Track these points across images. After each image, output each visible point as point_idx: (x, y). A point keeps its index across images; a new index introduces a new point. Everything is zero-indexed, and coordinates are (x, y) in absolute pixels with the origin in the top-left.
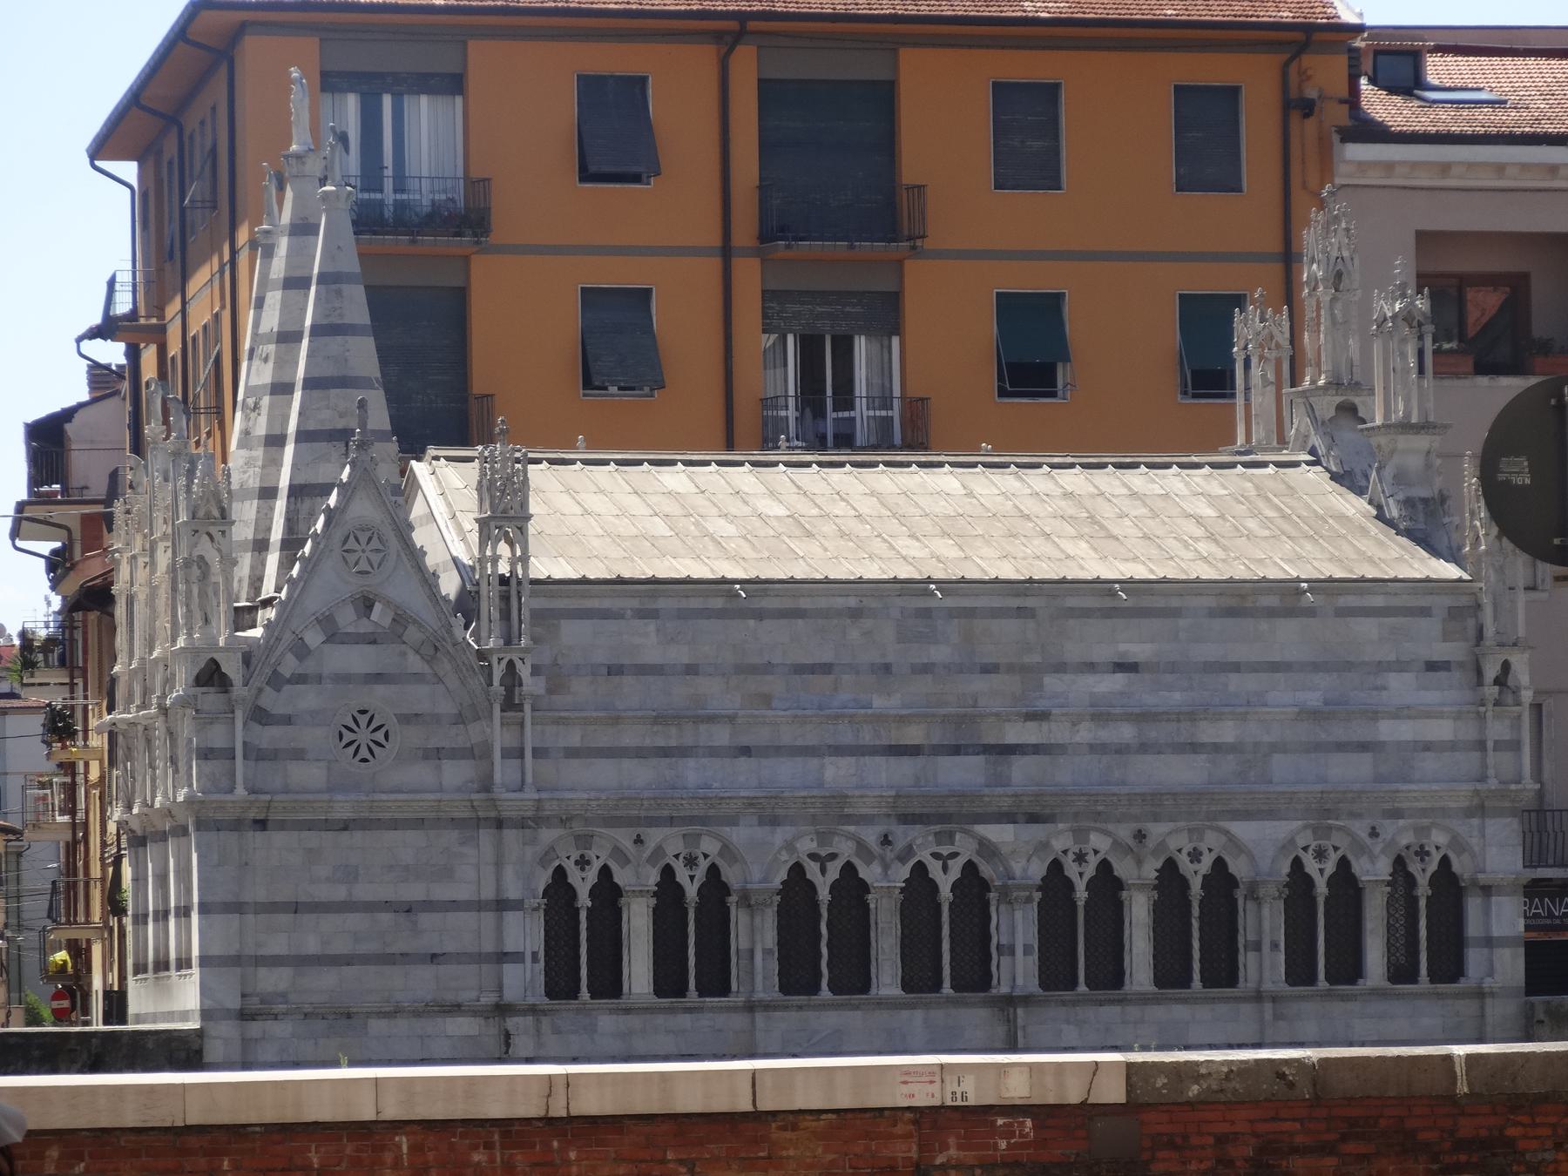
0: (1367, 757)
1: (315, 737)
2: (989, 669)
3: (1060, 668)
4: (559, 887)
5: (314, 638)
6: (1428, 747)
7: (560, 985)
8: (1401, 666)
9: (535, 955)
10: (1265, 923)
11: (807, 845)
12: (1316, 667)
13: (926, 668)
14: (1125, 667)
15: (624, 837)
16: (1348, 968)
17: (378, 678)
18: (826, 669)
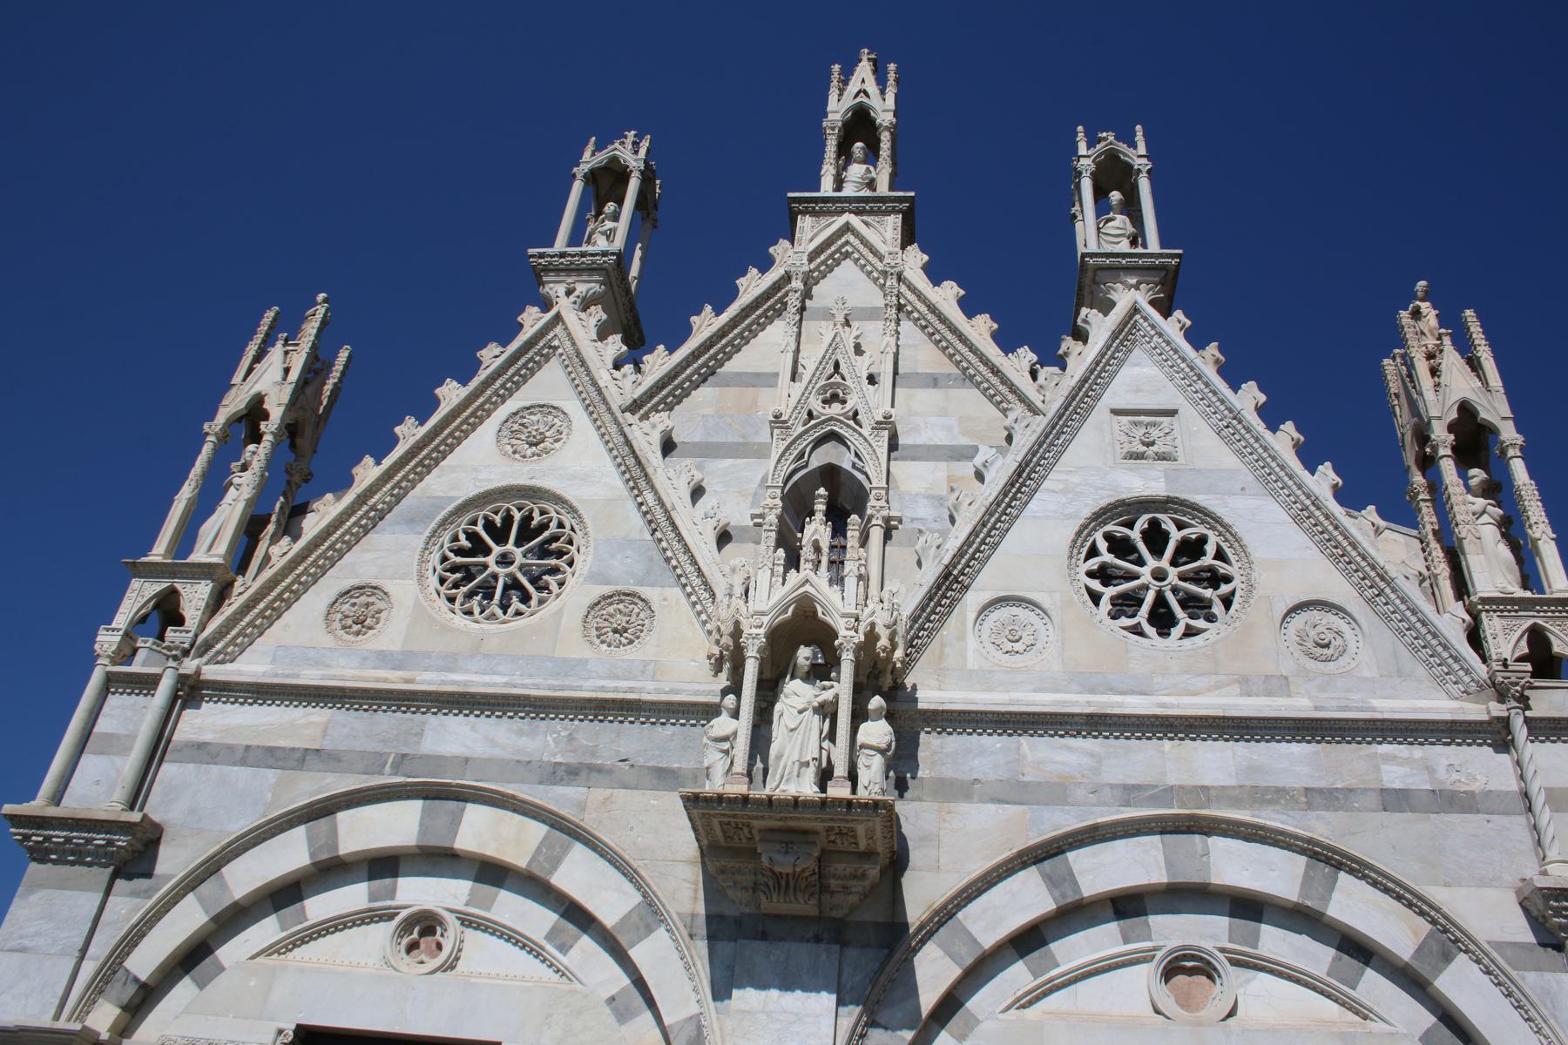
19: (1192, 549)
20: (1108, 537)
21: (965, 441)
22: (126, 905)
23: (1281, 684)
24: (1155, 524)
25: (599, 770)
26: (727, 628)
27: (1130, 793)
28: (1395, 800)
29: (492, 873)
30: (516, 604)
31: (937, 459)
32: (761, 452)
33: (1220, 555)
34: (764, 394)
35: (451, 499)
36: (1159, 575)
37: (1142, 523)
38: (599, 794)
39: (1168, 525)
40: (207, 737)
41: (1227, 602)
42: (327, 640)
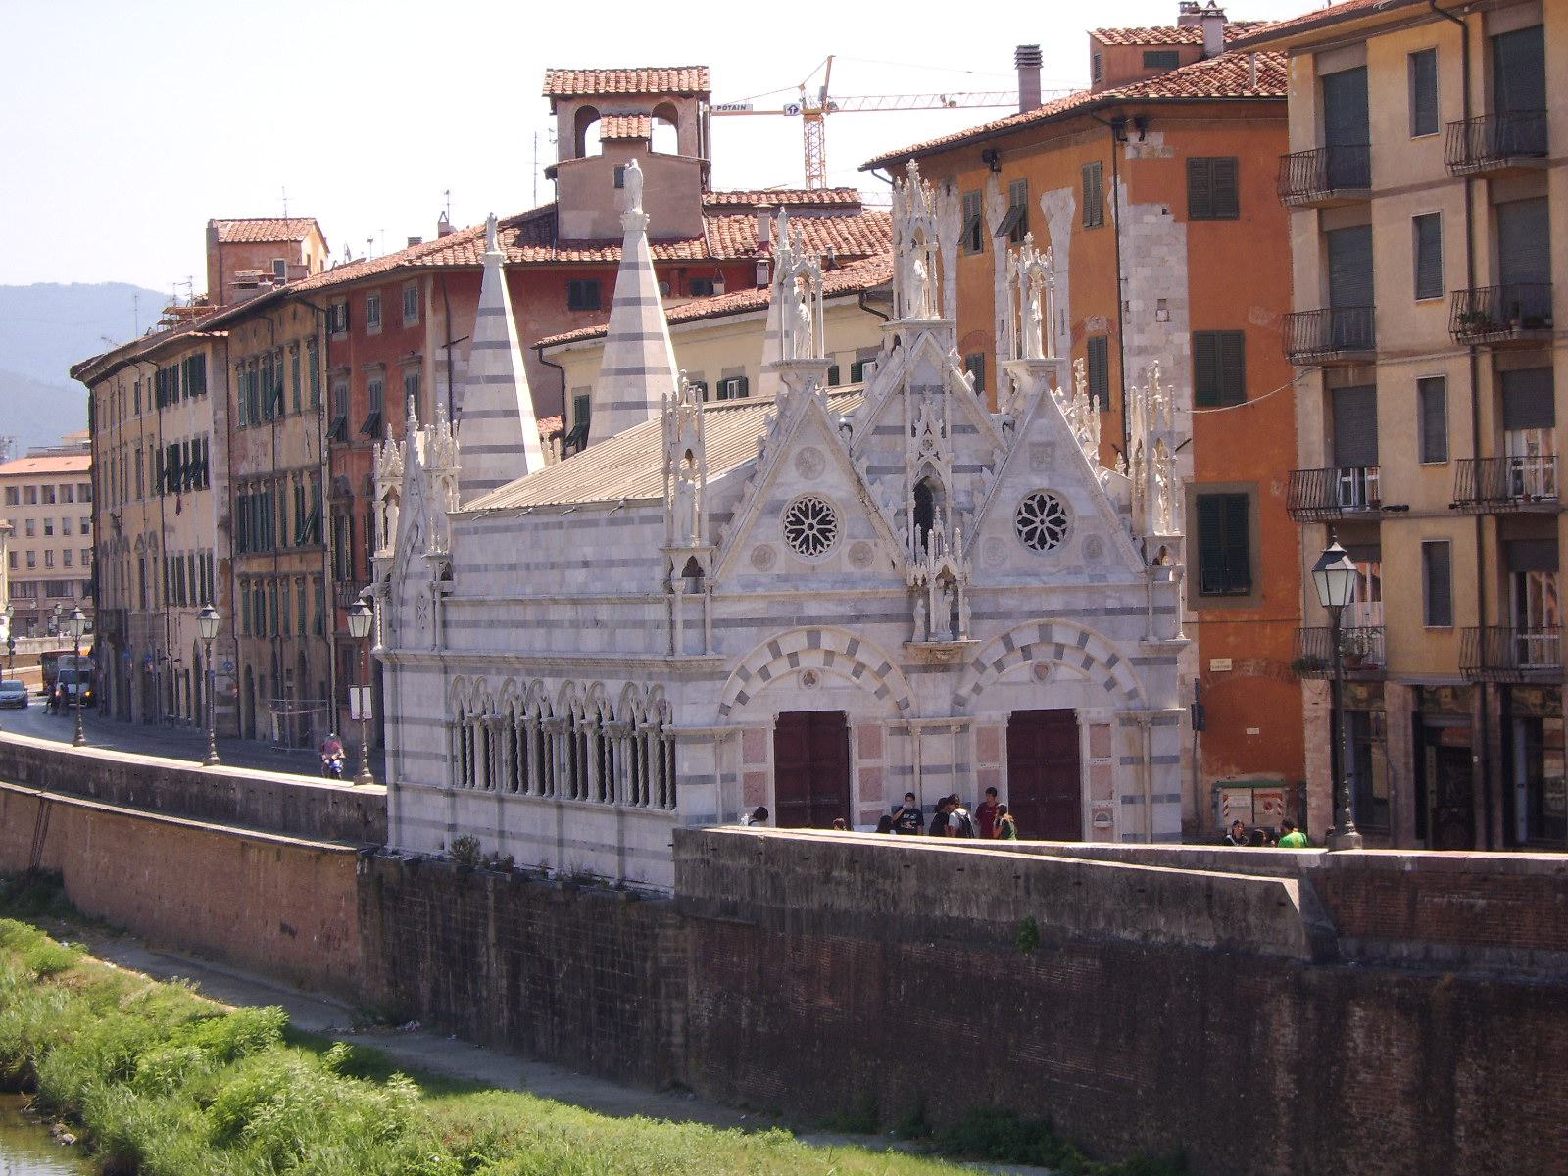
7: (467, 777)
9: (454, 758)
10: (623, 755)
14: (586, 564)
18: (512, 567)
19: (1054, 509)
20: (1026, 504)
21: (977, 462)
22: (719, 684)
23: (1077, 571)
24: (1042, 497)
25: (867, 616)
26: (920, 577)
27: (1032, 614)
28: (1110, 612)
29: (830, 654)
30: (819, 547)
31: (966, 472)
32: (904, 470)
33: (1063, 512)
34: (899, 438)
35: (785, 501)
36: (1042, 522)
37: (1037, 498)
38: (869, 626)
39: (1047, 499)
40: (726, 617)
41: (1064, 531)
42: (753, 571)
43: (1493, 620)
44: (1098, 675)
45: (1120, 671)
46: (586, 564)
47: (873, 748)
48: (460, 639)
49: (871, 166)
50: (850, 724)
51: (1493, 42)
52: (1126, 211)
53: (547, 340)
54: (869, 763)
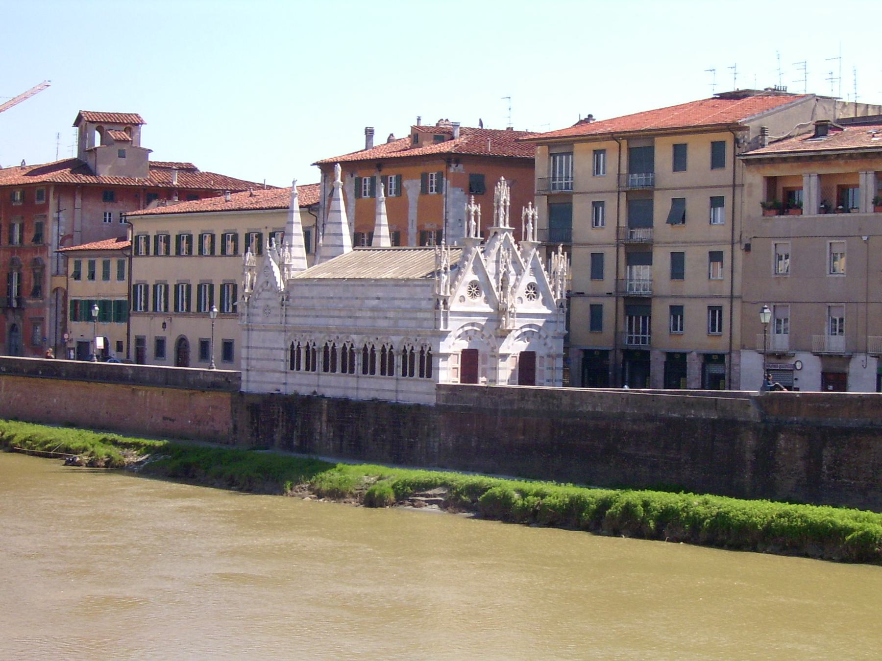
0: (414, 321)
1: (260, 311)
2: (357, 298)
3: (367, 298)
4: (292, 346)
5: (260, 290)
6: (425, 319)
7: (292, 368)
8: (424, 299)
9: (287, 361)
10: (398, 360)
11: (327, 338)
12: (409, 299)
13: (347, 298)
14: (378, 298)
15: (299, 335)
16: (412, 374)
17: (269, 299)
43: (621, 329)
44: (542, 341)
45: (548, 341)
46: (378, 298)
47: (484, 362)
48: (293, 321)
49: (314, 164)
50: (480, 353)
51: (630, 150)
52: (449, 189)
53: (129, 213)
54: (484, 366)
